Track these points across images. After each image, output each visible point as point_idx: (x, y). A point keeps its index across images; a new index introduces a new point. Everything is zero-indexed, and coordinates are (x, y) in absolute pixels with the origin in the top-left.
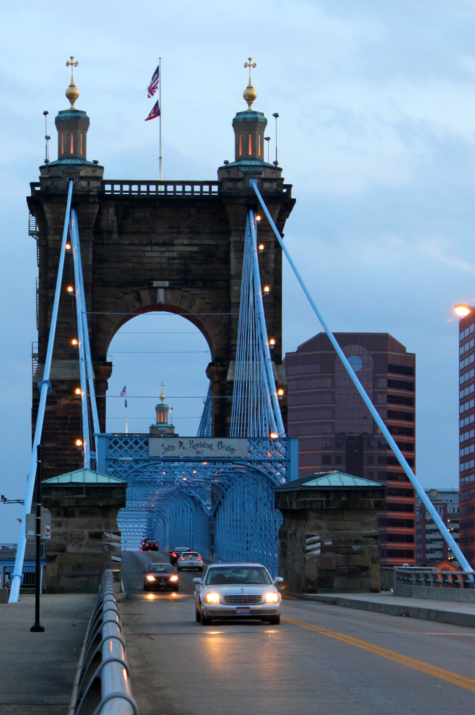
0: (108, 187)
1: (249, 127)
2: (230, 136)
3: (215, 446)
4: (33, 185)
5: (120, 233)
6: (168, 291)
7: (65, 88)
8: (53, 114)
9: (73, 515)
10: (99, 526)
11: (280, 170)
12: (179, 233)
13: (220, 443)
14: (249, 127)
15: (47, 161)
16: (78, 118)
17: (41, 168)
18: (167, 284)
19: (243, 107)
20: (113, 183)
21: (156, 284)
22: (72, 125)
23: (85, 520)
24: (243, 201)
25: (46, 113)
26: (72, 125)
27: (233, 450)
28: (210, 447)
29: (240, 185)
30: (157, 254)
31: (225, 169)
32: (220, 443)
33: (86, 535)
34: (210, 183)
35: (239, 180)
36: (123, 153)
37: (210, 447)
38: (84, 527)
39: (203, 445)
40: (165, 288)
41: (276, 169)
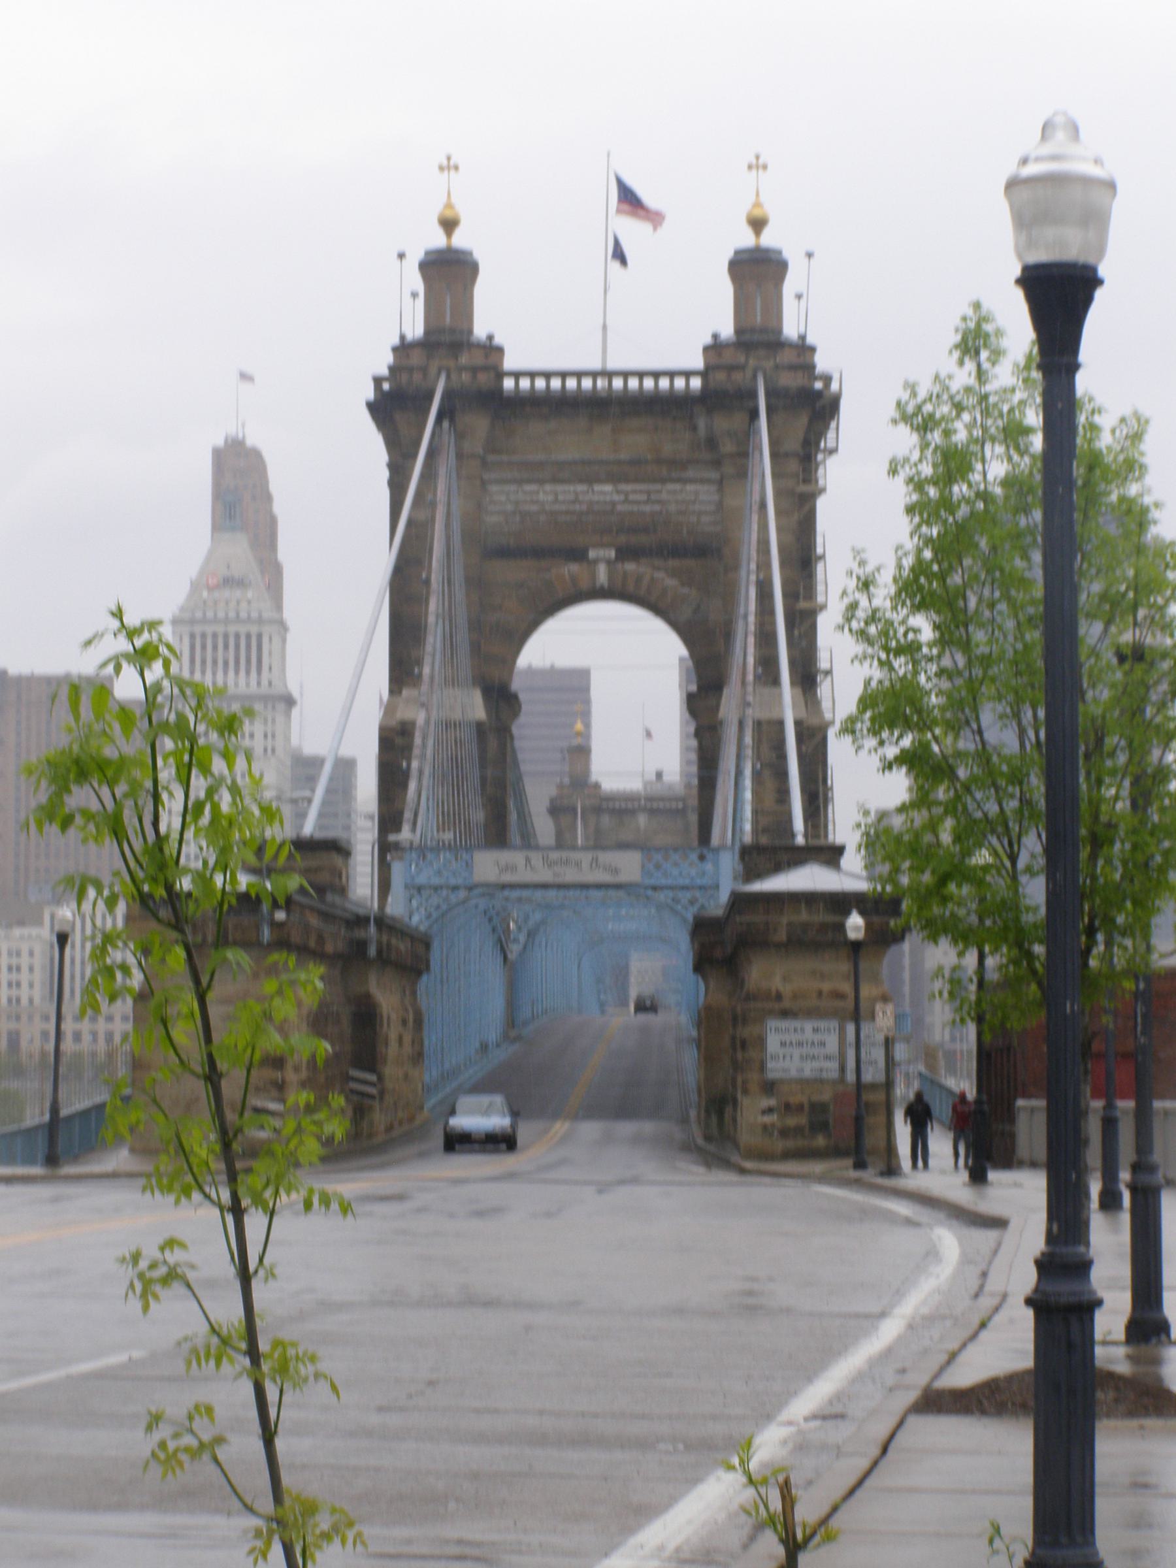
0: (508, 384)
2: (724, 292)
4: (378, 381)
8: (415, 256)
11: (813, 350)
15: (402, 337)
17: (395, 350)
19: (747, 239)
20: (517, 375)
22: (449, 273)
25: (401, 256)
26: (449, 273)
27: (615, 871)
31: (715, 348)
34: (687, 374)
39: (567, 862)
41: (804, 349)
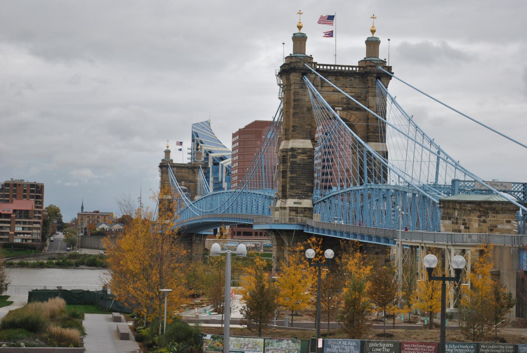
1: (373, 44)
3: (500, 186)
5: (322, 86)
6: (341, 112)
7: (296, 24)
9: (499, 214)
10: (509, 218)
12: (346, 87)
13: (502, 184)
14: (373, 44)
16: (304, 36)
18: (341, 108)
20: (320, 65)
21: (336, 108)
23: (503, 216)
24: (375, 75)
27: (506, 187)
28: (498, 185)
29: (373, 68)
30: (337, 96)
32: (502, 184)
33: (505, 221)
35: (374, 66)
36: (321, 51)
37: (498, 185)
38: (504, 218)
40: (340, 110)
